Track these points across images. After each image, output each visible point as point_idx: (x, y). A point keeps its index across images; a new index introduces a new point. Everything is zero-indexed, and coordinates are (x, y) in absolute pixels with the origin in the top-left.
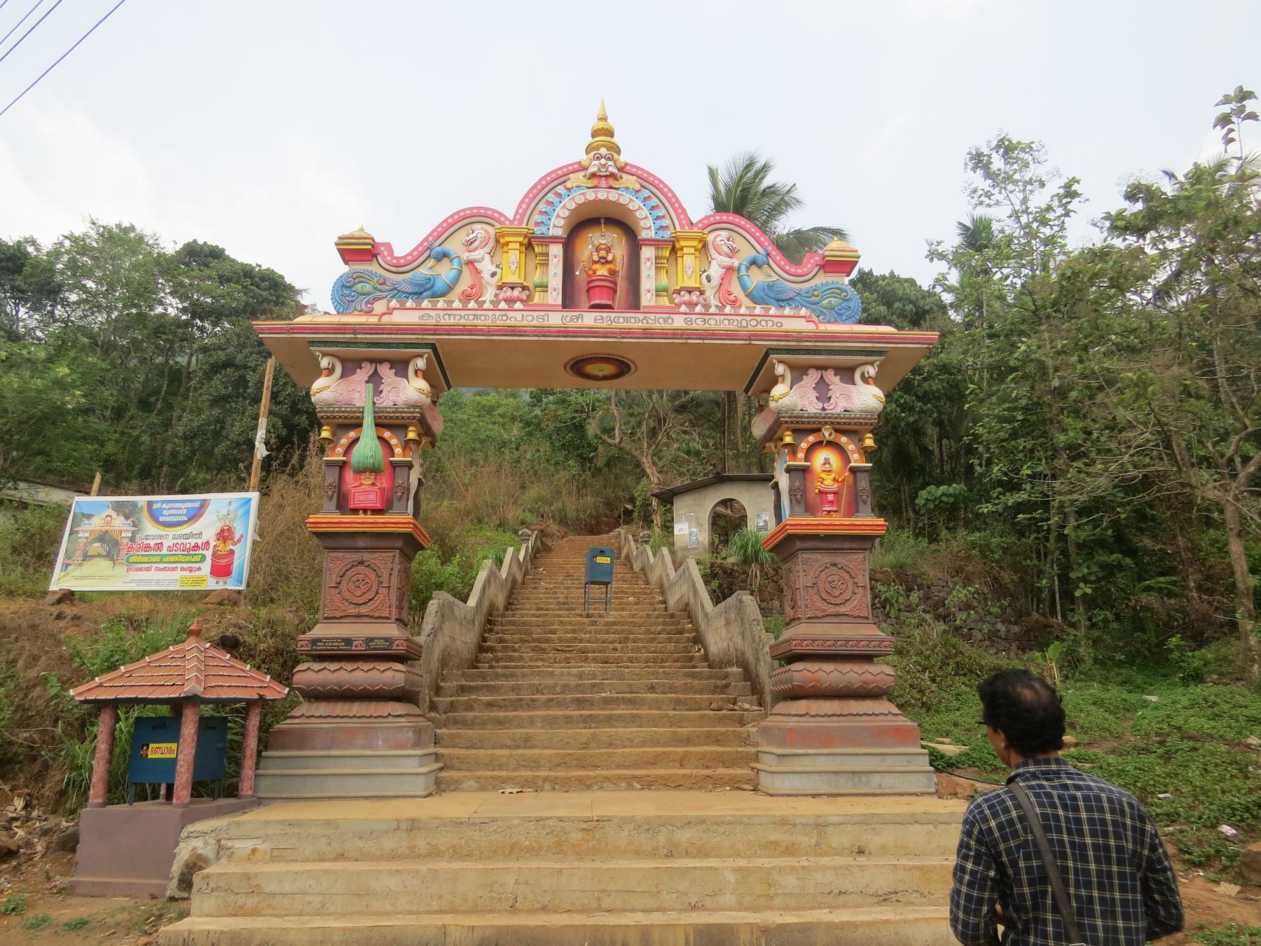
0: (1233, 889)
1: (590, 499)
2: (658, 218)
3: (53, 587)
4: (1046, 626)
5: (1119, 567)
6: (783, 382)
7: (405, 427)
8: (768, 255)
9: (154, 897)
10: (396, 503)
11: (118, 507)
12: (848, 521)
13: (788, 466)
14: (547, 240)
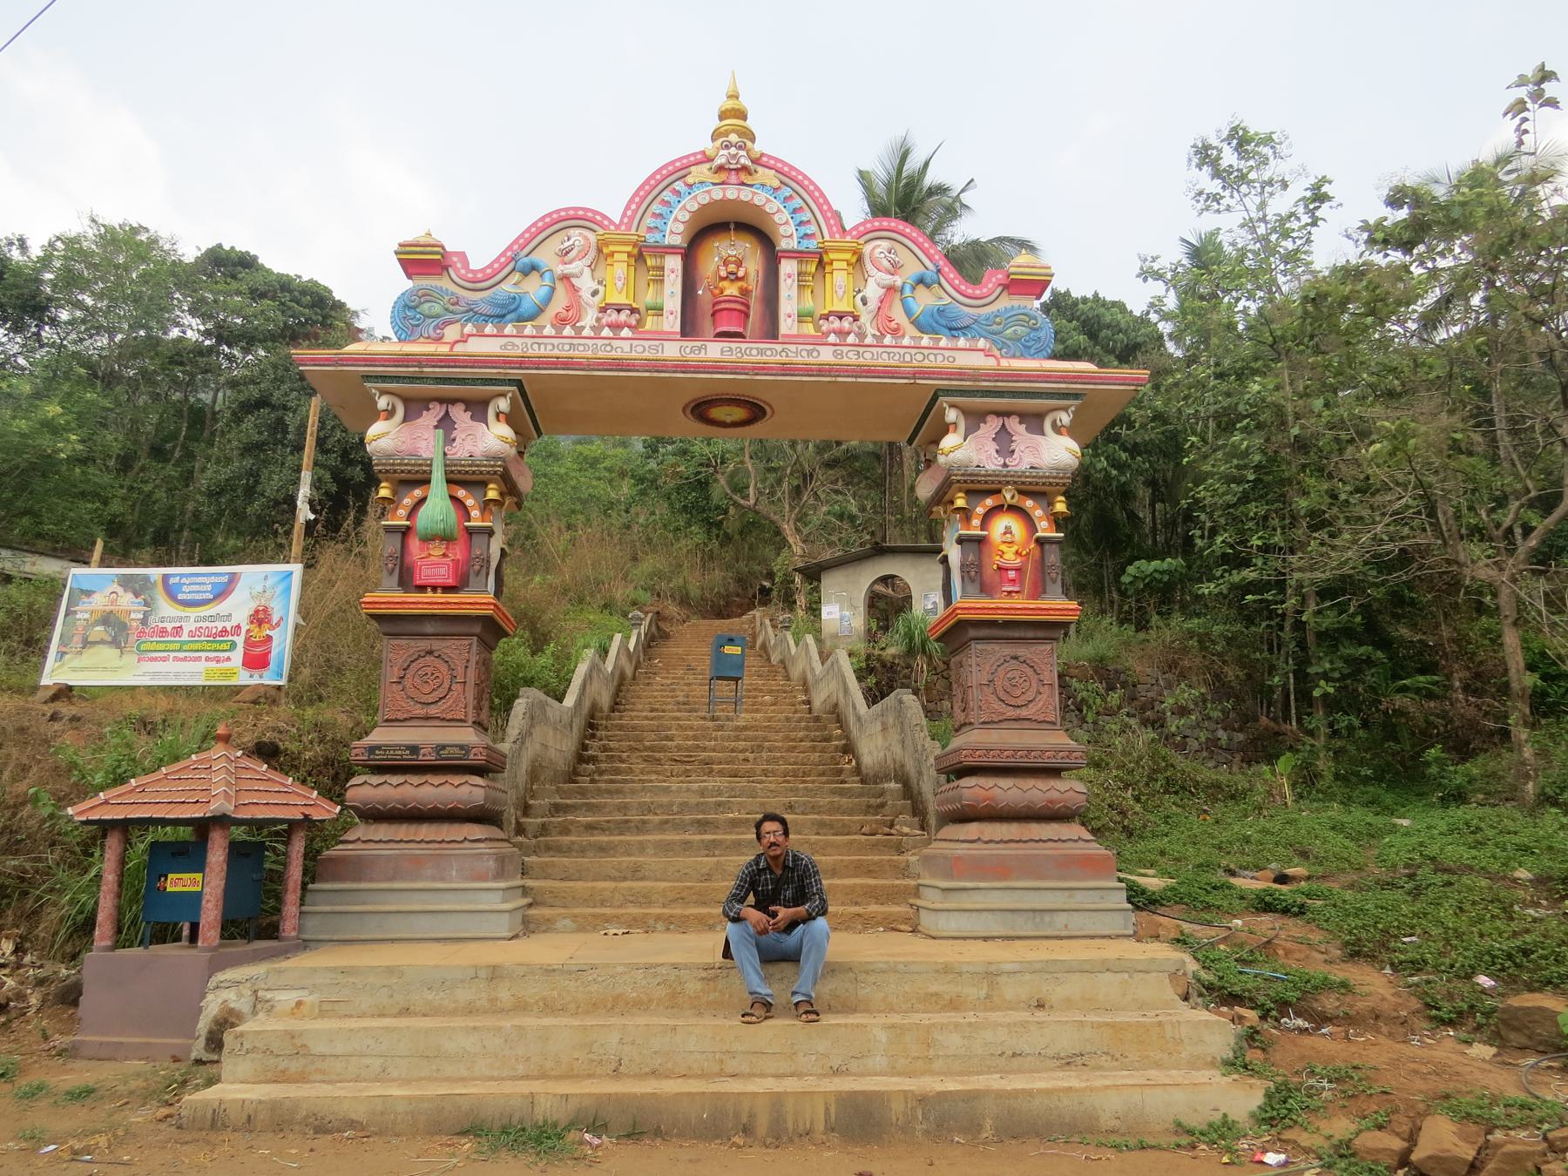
0: (1487, 1051)
2: (801, 223)
4: (1278, 734)
5: (1369, 662)
6: (955, 431)
7: (483, 484)
8: (939, 271)
9: (176, 1060)
10: (472, 579)
11: (126, 582)
12: (1033, 604)
13: (960, 535)
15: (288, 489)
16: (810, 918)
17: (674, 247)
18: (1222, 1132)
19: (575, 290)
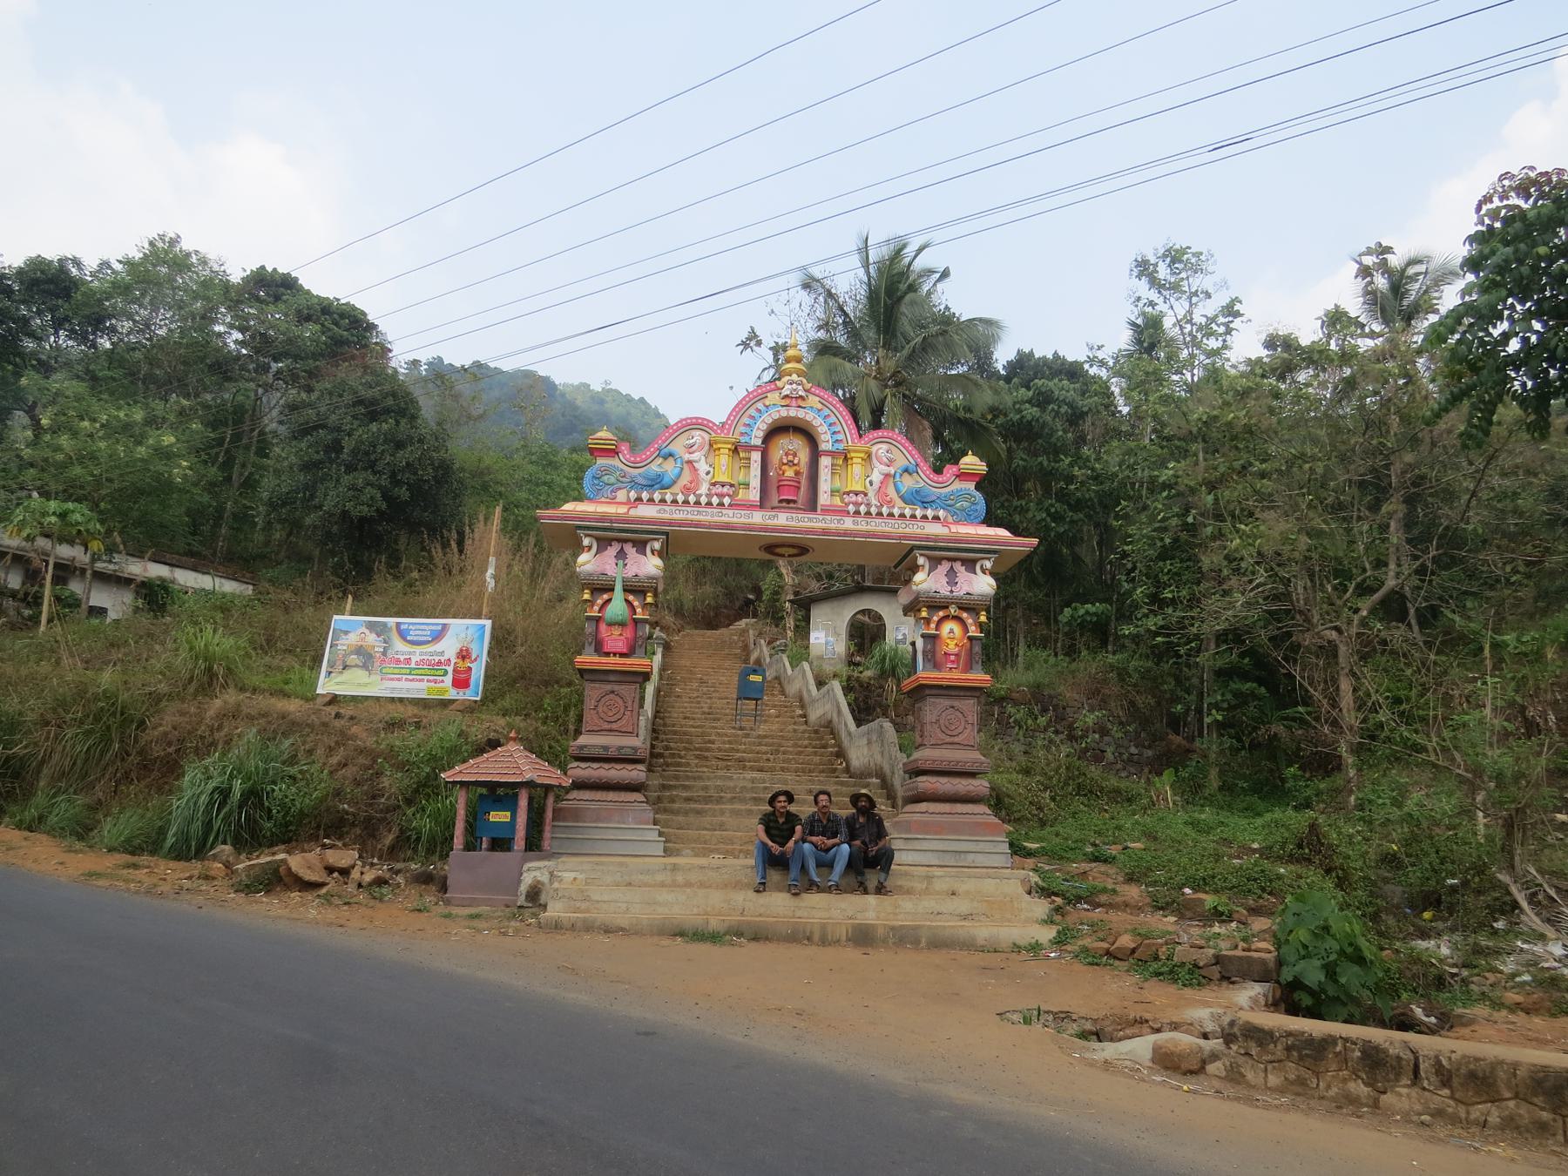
0: (1172, 919)
1: (708, 589)
2: (834, 433)
4: (1188, 751)
5: (1253, 695)
9: (508, 906)
11: (371, 626)
12: (964, 676)
14: (750, 448)
16: (838, 845)
17: (757, 446)
18: (1035, 948)
19: (696, 470)
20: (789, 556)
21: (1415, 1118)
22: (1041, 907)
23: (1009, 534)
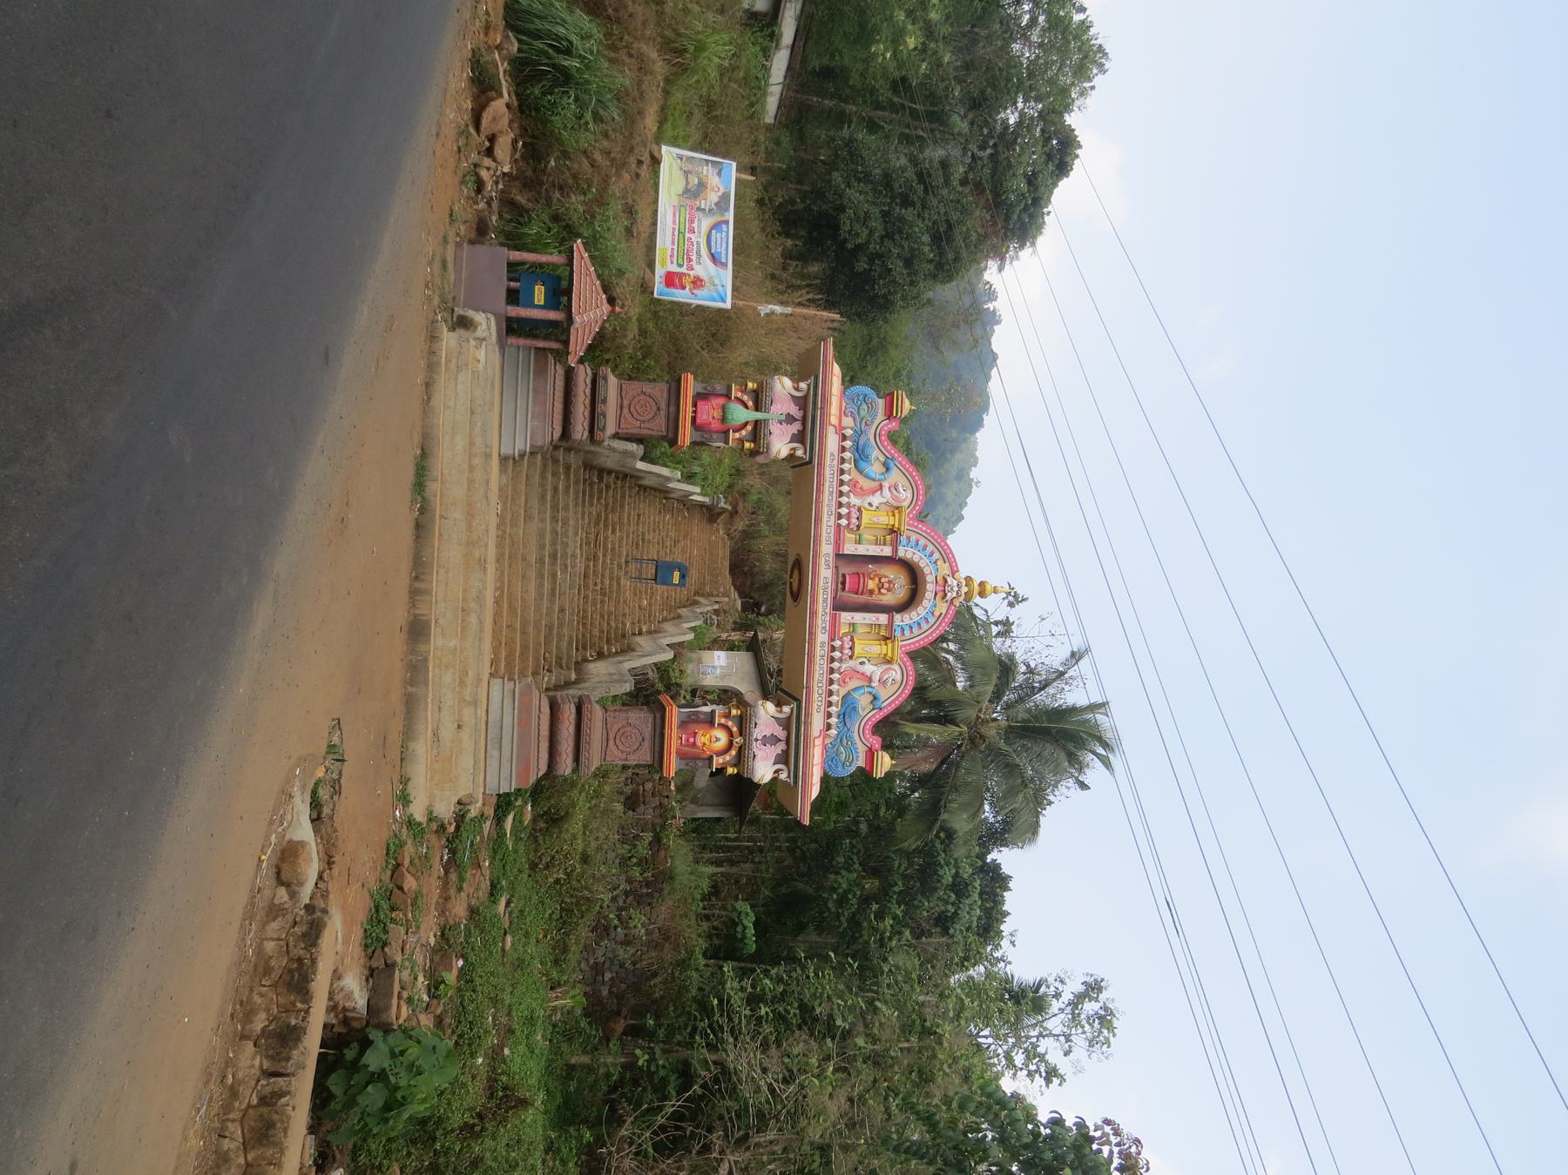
2: (911, 628)
3: (664, 148)
9: (454, 298)
11: (725, 197)
12: (673, 750)
15: (850, 208)
17: (896, 552)
18: (405, 800)
19: (873, 492)
20: (791, 583)
21: (230, 1070)
22: (445, 811)
23: (813, 798)
